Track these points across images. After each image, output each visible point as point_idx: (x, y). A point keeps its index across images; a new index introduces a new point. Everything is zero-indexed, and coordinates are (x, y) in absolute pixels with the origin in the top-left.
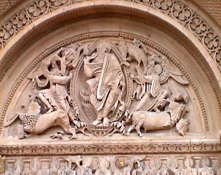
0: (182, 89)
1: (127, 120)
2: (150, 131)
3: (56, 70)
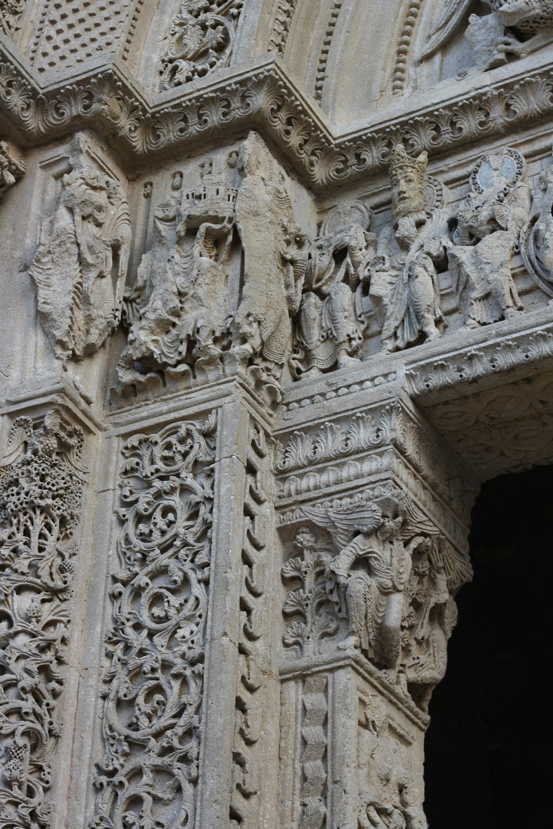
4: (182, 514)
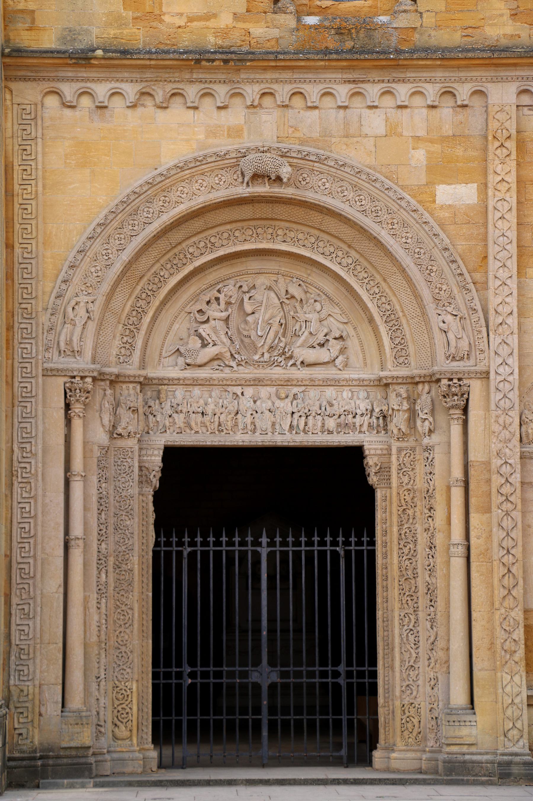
0: (341, 326)
1: (288, 355)
2: (309, 365)
3: (214, 305)
4: (127, 467)
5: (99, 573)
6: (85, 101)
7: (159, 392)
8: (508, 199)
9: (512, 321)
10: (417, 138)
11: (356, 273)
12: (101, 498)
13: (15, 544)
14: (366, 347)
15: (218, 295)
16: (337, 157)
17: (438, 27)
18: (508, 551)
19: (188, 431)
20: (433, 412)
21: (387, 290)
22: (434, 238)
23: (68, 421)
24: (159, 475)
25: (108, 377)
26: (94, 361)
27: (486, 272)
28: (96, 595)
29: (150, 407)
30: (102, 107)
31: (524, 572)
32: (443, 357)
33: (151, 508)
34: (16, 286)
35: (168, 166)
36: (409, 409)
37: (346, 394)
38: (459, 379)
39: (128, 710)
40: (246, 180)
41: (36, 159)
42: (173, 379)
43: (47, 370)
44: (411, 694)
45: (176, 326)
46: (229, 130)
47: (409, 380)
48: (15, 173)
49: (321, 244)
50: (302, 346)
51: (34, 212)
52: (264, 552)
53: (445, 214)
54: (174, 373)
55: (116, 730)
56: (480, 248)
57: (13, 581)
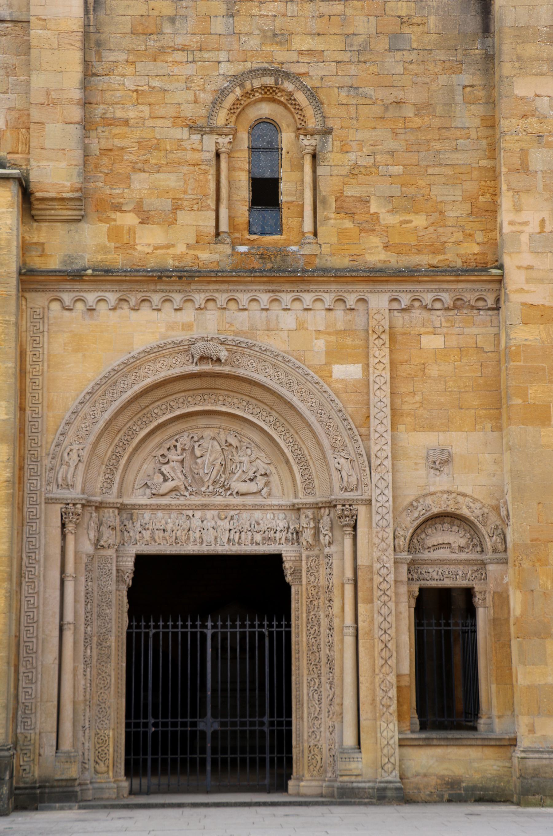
0: (266, 466)
1: (226, 487)
2: (243, 495)
3: (173, 451)
5: (86, 649)
6: (80, 306)
7: (132, 515)
8: (383, 375)
9: (388, 463)
10: (318, 332)
11: (276, 427)
12: (87, 593)
13: (22, 627)
14: (284, 481)
15: (176, 444)
16: (261, 344)
17: (332, 254)
18: (385, 631)
19: (153, 543)
20: (331, 529)
21: (299, 440)
22: (331, 402)
23: (64, 536)
24: (132, 575)
25: (94, 504)
26: (83, 492)
27: (369, 427)
28: (82, 666)
29: (125, 525)
30: (91, 310)
31: (397, 647)
32: (338, 489)
33: (125, 600)
34: (27, 438)
35: (138, 351)
36: (315, 527)
37: (269, 515)
38: (350, 505)
39: (106, 751)
40: (195, 360)
41: (42, 347)
42: (142, 505)
43: (48, 499)
44: (316, 738)
45: (145, 466)
46: (183, 325)
47: (315, 506)
48: (28, 356)
49: (250, 407)
50: (237, 480)
51: (41, 384)
52: (209, 632)
53: (339, 386)
54: (143, 501)
55: (97, 766)
56: (364, 410)
57: (21, 655)
